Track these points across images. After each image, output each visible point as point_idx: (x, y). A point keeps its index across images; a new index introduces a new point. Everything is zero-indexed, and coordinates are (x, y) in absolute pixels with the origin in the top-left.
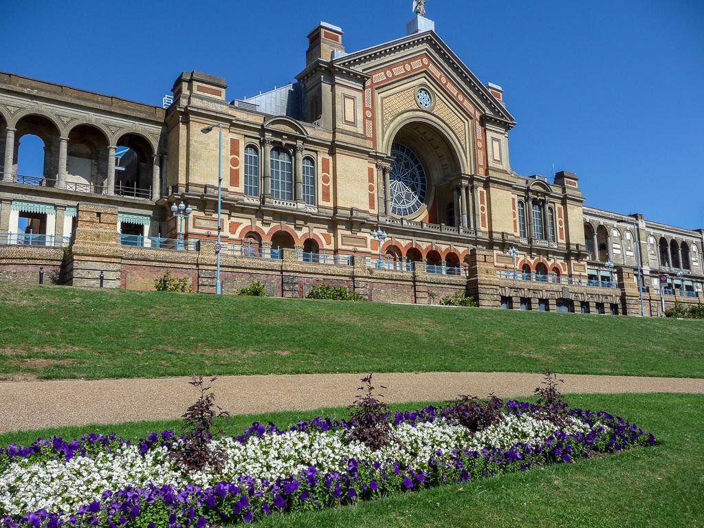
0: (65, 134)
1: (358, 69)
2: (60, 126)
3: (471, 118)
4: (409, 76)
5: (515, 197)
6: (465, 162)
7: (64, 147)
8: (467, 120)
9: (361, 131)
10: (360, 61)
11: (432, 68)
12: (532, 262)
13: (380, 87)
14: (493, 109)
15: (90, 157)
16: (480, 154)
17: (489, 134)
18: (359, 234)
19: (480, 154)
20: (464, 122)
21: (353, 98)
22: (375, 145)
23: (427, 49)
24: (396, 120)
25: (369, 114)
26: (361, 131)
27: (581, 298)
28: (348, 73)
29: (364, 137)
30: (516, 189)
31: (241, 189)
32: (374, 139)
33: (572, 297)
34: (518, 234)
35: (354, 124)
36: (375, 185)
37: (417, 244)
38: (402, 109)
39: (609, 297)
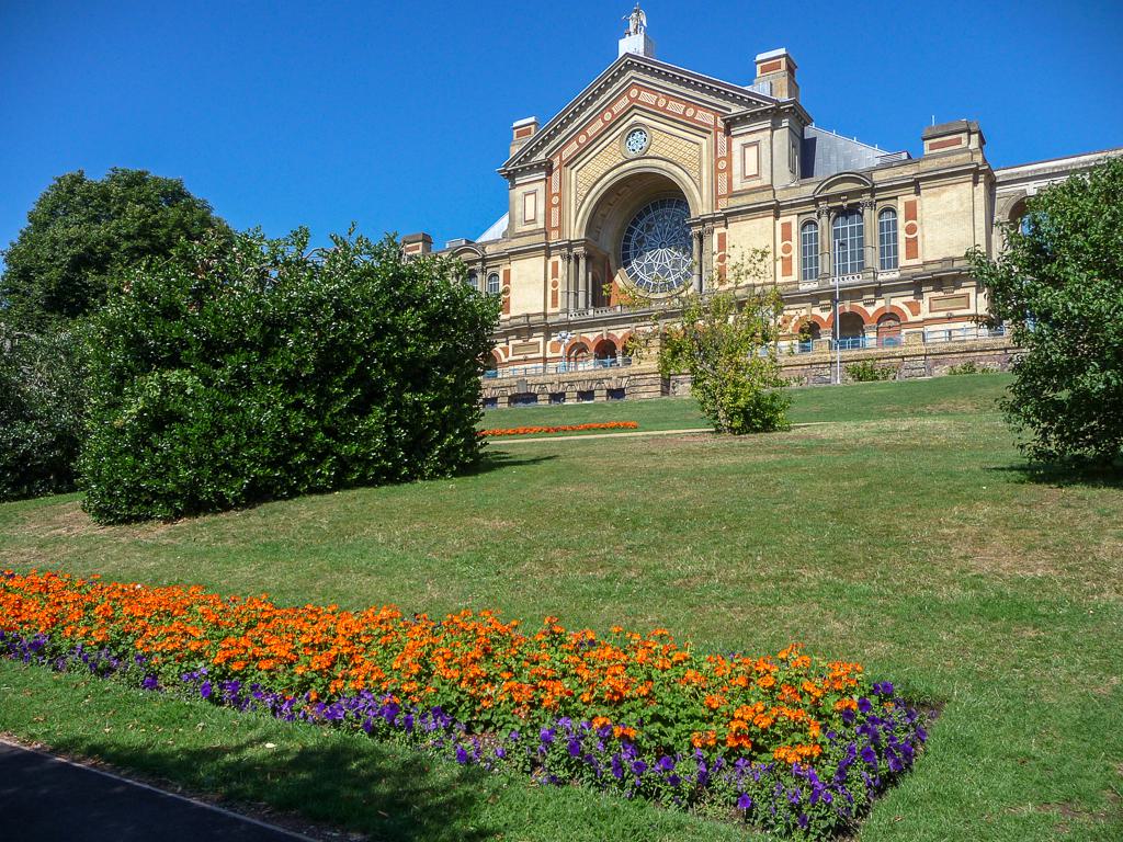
1: (541, 156)
3: (709, 132)
4: (609, 127)
6: (698, 200)
10: (539, 148)
11: (646, 97)
12: (825, 315)
14: (741, 102)
18: (531, 340)
23: (632, 77)
27: (549, 389)
28: (531, 167)
30: (793, 206)
33: (535, 390)
35: (534, 221)
36: (559, 280)
37: (608, 335)
39: (605, 381)
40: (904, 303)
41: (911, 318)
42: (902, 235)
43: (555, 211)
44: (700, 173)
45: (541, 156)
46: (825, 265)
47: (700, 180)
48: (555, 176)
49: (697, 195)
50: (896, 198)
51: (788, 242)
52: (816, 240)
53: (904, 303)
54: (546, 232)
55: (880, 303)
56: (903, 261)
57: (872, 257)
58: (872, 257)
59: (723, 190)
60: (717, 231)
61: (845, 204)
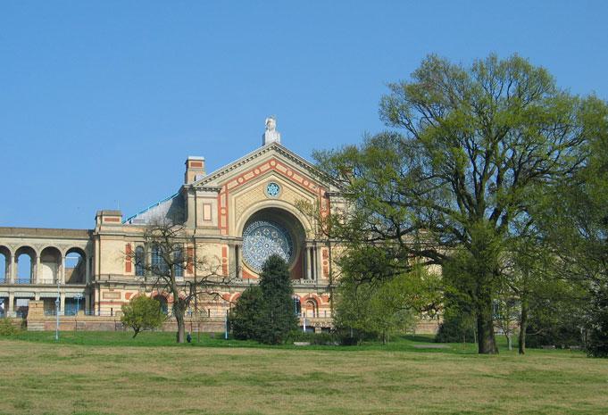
0: (38, 254)
2: (36, 250)
4: (257, 177)
7: (39, 259)
9: (216, 225)
13: (234, 189)
15: (55, 262)
21: (210, 204)
22: (227, 233)
24: (247, 211)
25: (223, 211)
26: (216, 225)
29: (219, 228)
31: (133, 272)
32: (227, 228)
38: (253, 202)
43: (223, 218)
45: (214, 184)
48: (223, 197)
54: (219, 228)
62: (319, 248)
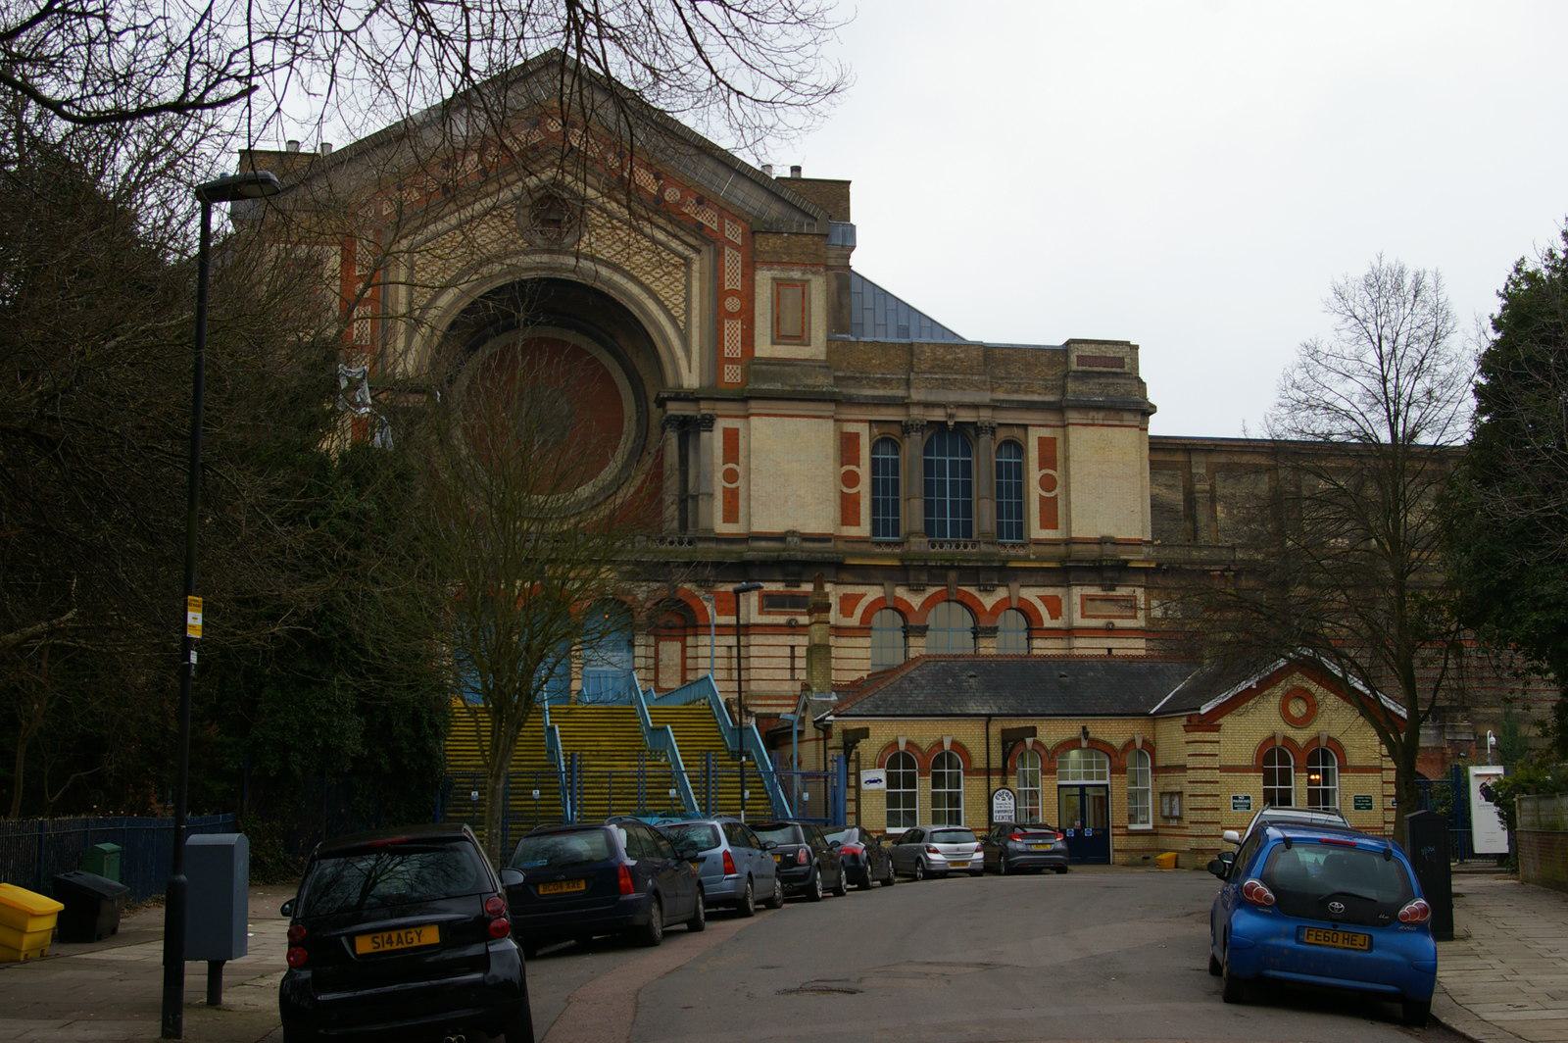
5: (863, 430)
8: (698, 251)
16: (733, 330)
17: (764, 278)
19: (733, 330)
20: (685, 258)
34: (864, 529)
40: (1040, 597)
41: (1048, 623)
42: (1034, 492)
44: (688, 312)
46: (912, 514)
47: (688, 323)
49: (680, 353)
50: (1025, 427)
51: (852, 468)
52: (896, 472)
53: (1040, 597)
55: (1002, 593)
56: (1036, 531)
57: (985, 515)
58: (985, 515)
59: (732, 347)
60: (721, 424)
61: (951, 423)
62: (708, 422)
